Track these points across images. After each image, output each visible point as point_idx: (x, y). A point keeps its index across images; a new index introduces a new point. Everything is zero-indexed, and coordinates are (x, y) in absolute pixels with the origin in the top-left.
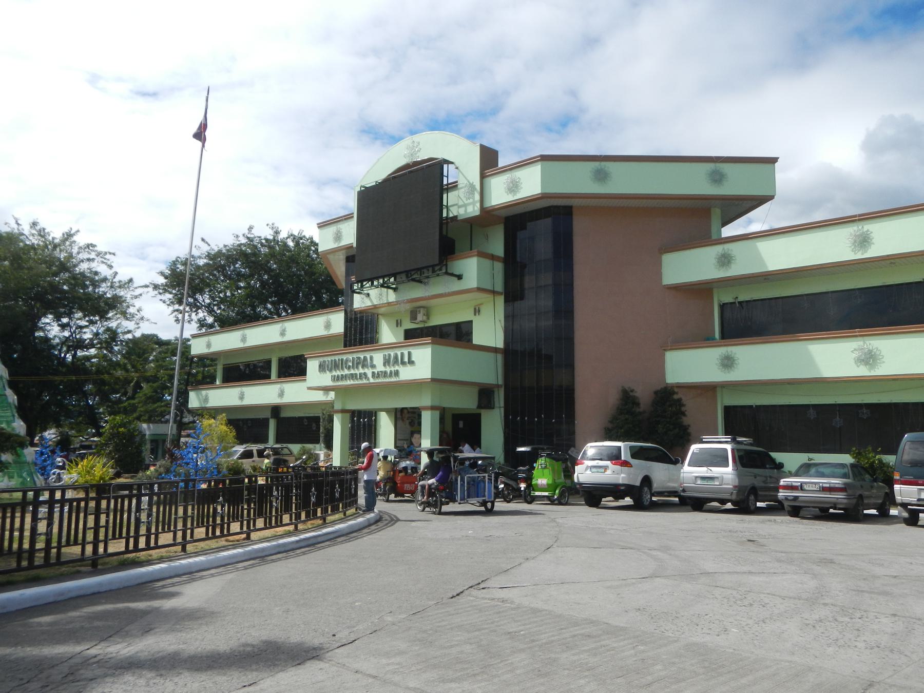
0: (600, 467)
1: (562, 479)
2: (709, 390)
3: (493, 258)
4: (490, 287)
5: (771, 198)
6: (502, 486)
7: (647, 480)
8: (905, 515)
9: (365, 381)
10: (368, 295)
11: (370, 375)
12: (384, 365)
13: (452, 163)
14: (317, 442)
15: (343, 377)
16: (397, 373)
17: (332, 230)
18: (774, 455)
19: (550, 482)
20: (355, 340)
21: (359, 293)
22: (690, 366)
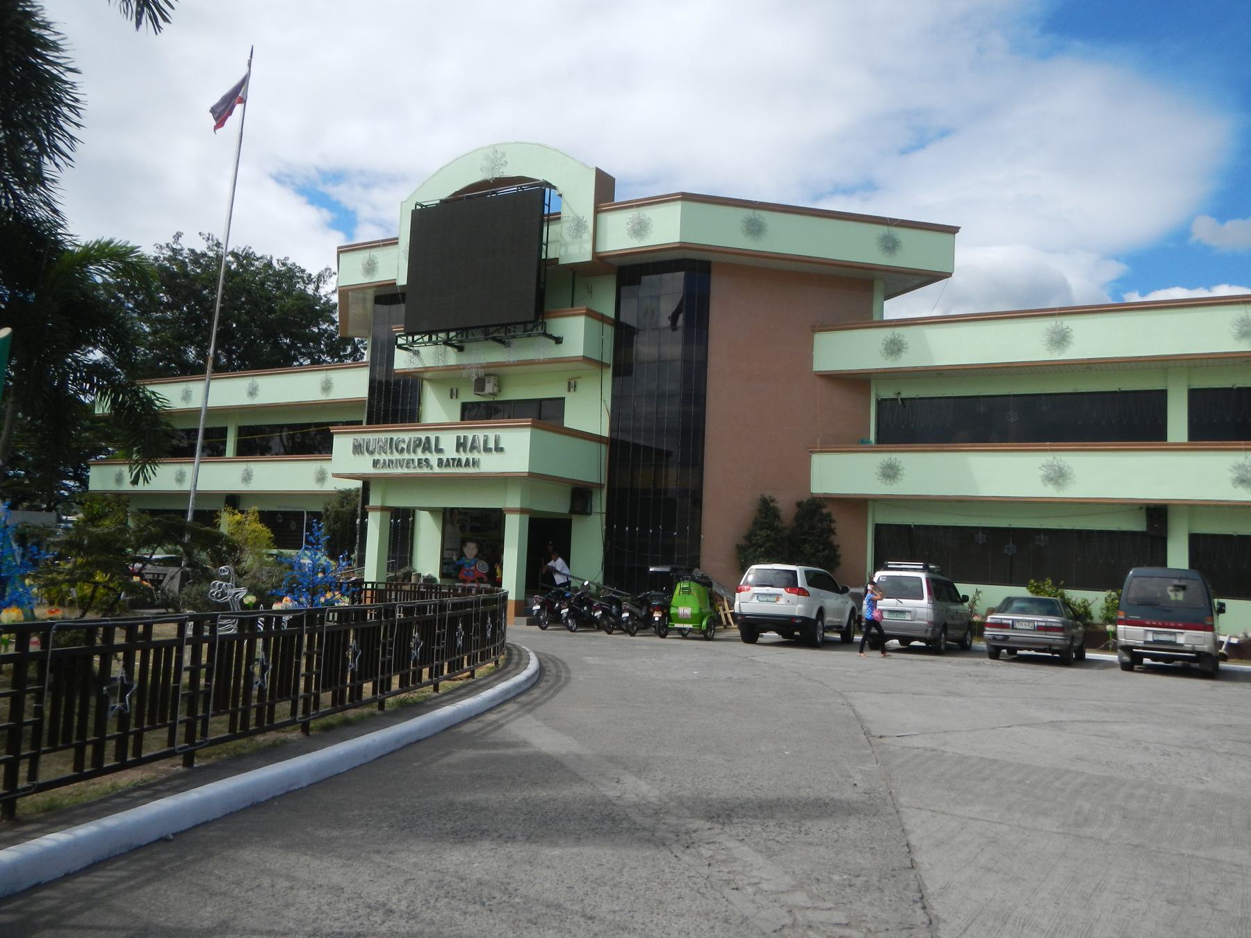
0: (771, 595)
1: (708, 609)
2: (858, 505)
3: (602, 318)
4: (597, 357)
5: (947, 275)
6: (626, 615)
7: (821, 612)
8: (1126, 658)
9: (425, 470)
10: (417, 353)
11: (434, 462)
12: (458, 450)
13: (555, 188)
14: (300, 548)
16: (475, 463)
17: (361, 257)
18: (958, 586)
19: (696, 611)
20: (386, 412)
21: (406, 349)
22: (841, 474)
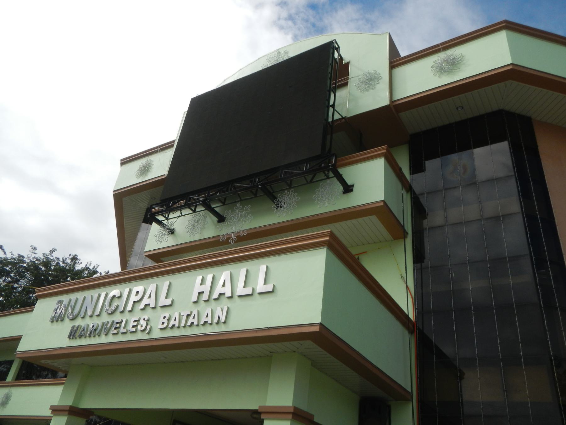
15: (95, 332)
